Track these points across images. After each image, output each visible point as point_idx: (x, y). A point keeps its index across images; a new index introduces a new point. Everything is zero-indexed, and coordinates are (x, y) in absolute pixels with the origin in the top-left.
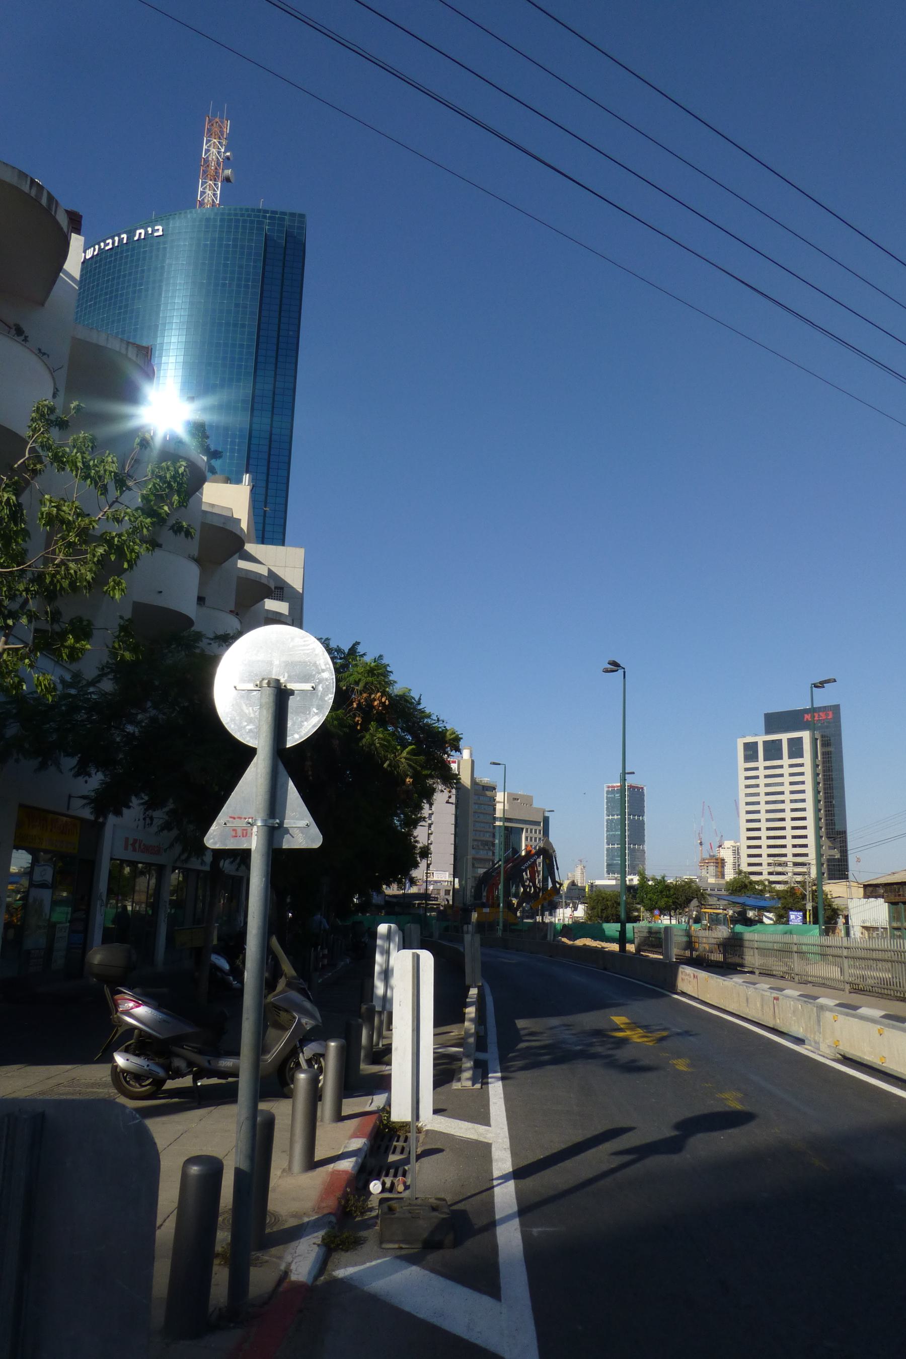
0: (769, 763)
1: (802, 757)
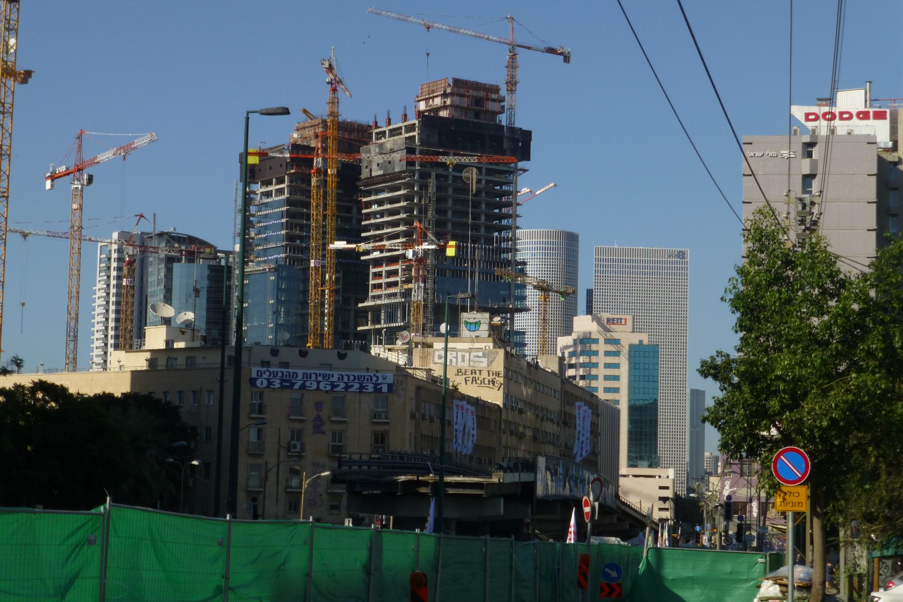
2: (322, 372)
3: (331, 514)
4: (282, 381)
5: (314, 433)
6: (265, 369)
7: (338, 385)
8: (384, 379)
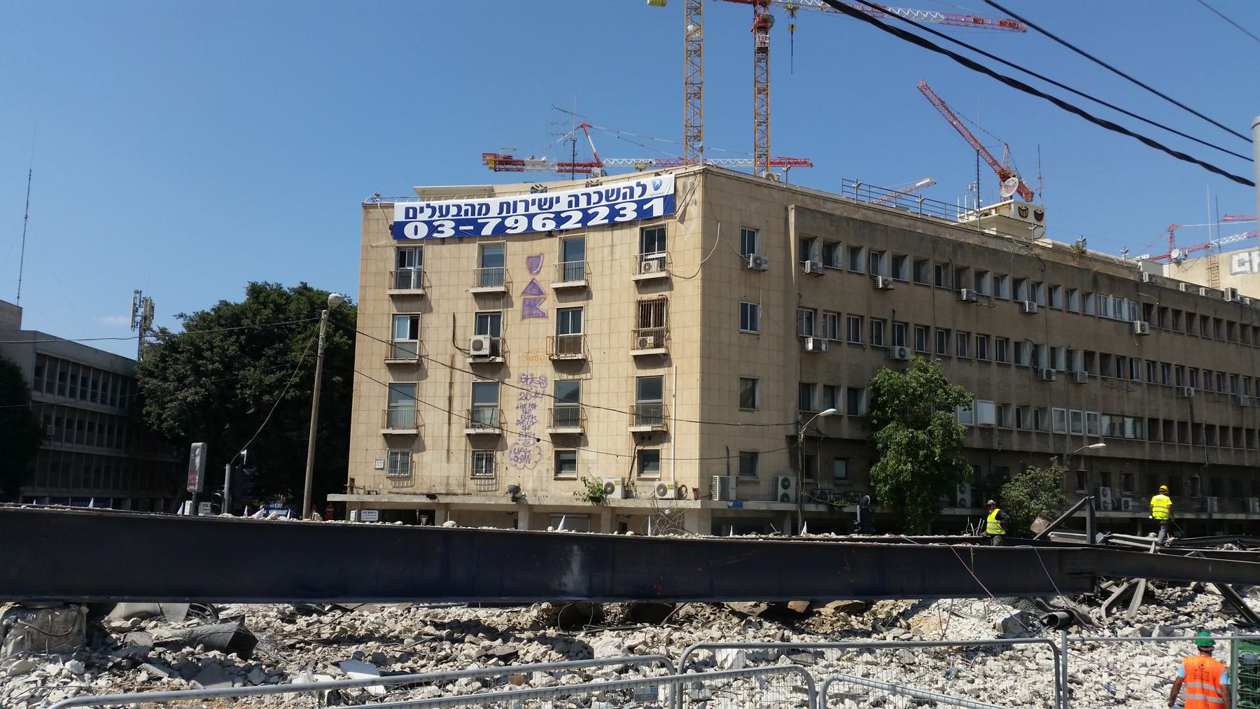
4: (459, 223)
5: (523, 317)
6: (424, 204)
7: (569, 217)
8: (656, 188)
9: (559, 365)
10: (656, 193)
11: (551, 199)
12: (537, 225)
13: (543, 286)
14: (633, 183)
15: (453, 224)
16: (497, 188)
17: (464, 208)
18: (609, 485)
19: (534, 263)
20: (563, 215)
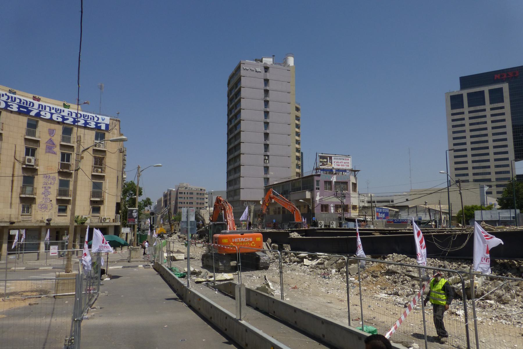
0: (472, 109)
1: (502, 101)
2: (55, 107)
3: (59, 216)
4: (20, 107)
5: (46, 152)
7: (68, 119)
8: (103, 120)
9: (60, 173)
10: (103, 122)
11: (61, 110)
12: (55, 117)
13: (55, 142)
14: (94, 115)
15: (17, 106)
16: (17, 92)
17: (22, 101)
18: (86, 218)
19: (51, 132)
20: (66, 117)
